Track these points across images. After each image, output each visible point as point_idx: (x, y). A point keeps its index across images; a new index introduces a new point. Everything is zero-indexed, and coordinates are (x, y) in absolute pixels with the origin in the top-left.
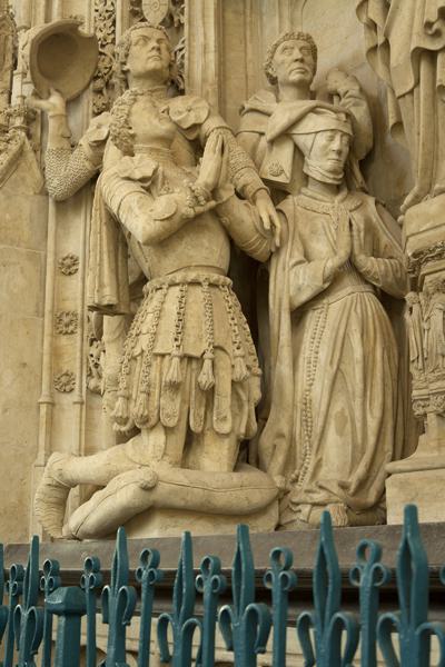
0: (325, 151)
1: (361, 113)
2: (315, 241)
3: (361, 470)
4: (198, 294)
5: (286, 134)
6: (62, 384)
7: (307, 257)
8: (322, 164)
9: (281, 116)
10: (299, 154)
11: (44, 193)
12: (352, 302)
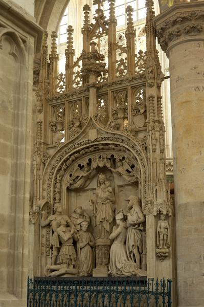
0: (85, 227)
1: (89, 220)
2: (84, 239)
3: (88, 269)
4: (70, 247)
5: (80, 224)
6: (42, 254)
7: (82, 242)
8: (84, 228)
9: (79, 221)
10: (81, 226)
11: (39, 225)
12: (88, 248)
